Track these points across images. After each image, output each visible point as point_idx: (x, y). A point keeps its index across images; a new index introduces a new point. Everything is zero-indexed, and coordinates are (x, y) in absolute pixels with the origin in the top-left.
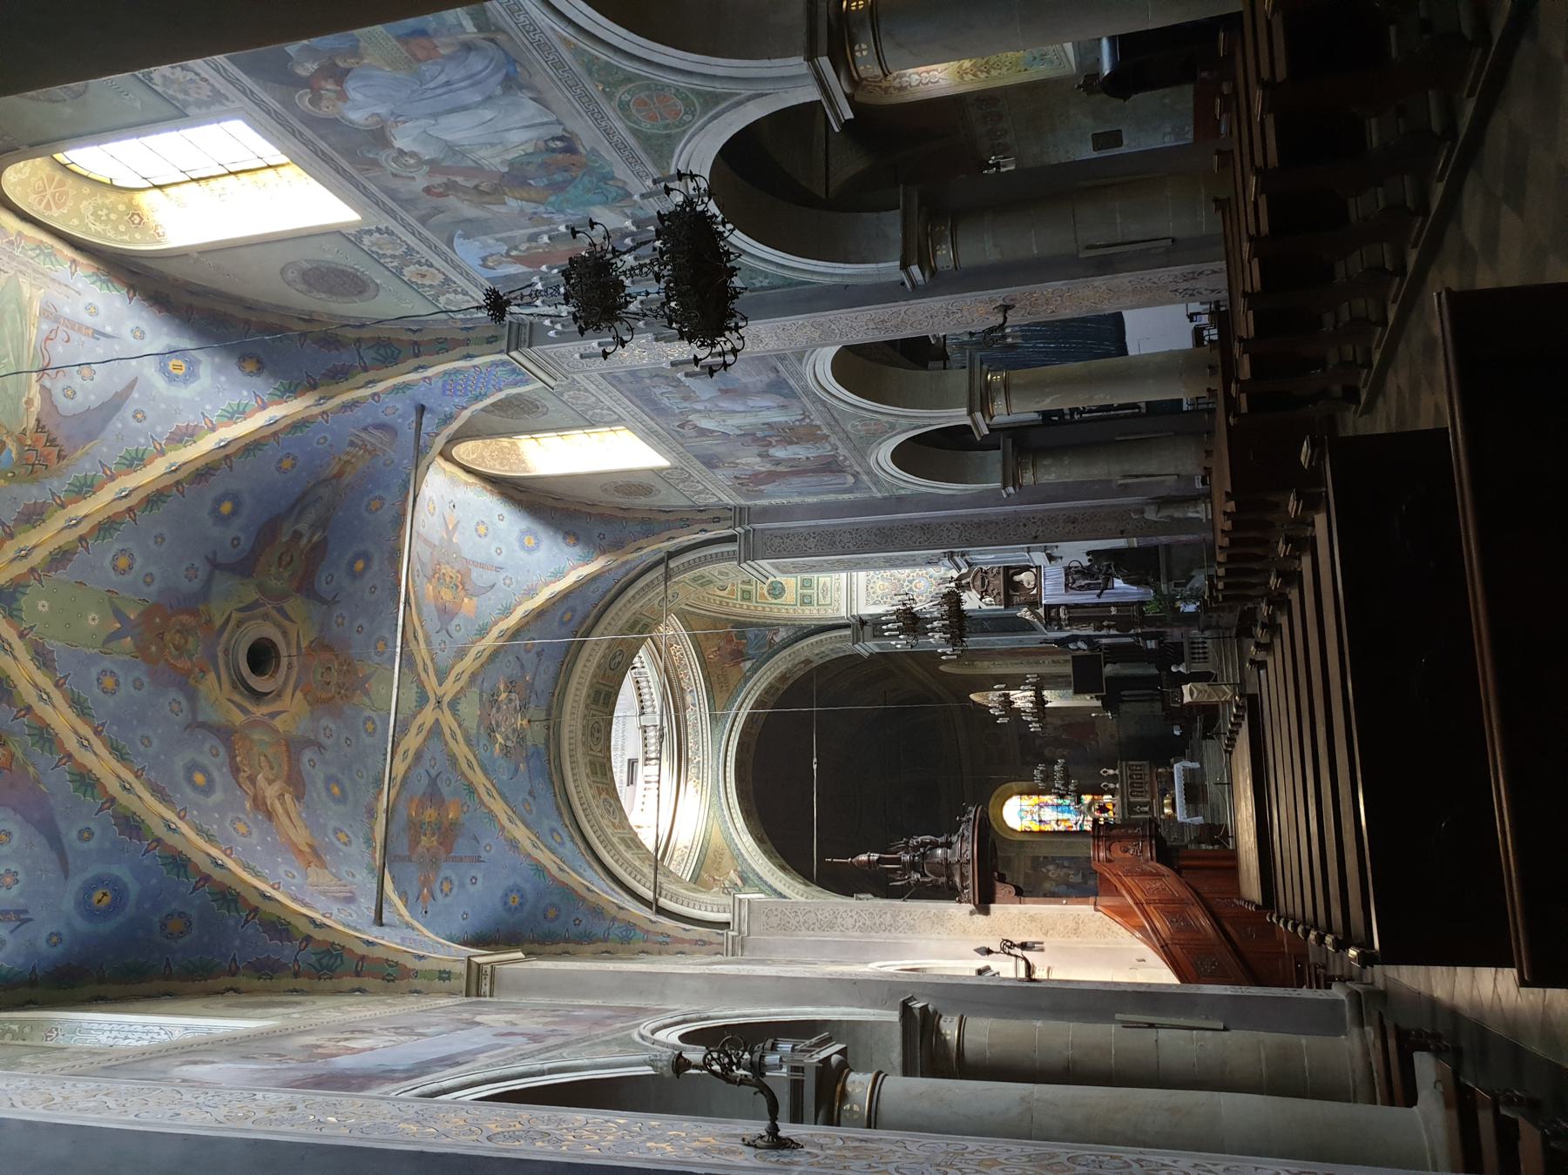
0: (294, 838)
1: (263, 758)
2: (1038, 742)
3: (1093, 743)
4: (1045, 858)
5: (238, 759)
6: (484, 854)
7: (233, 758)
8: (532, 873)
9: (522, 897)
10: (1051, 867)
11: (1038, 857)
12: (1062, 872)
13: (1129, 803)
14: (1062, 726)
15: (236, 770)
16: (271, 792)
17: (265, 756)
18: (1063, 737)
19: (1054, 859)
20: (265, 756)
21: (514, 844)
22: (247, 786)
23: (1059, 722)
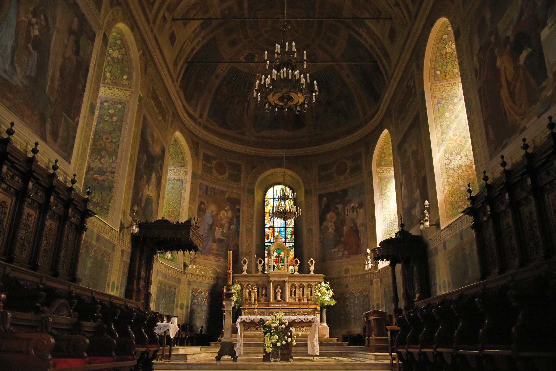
2: (340, 207)
3: (340, 254)
4: (239, 210)
10: (230, 214)
11: (239, 204)
12: (225, 222)
13: (284, 282)
14: (356, 225)
18: (345, 228)
19: (238, 217)
23: (359, 222)
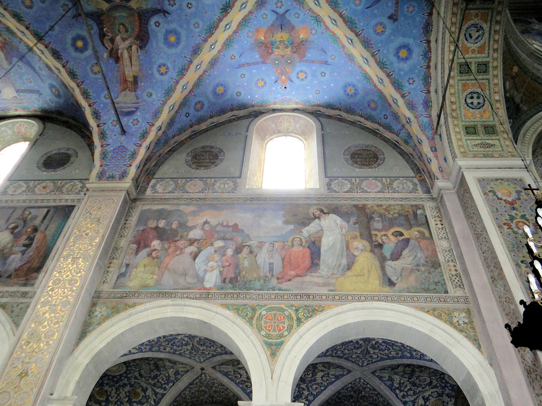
0: (126, 72)
1: (121, 26)
5: (105, 29)
6: (330, 61)
7: (101, 29)
8: (362, 78)
9: (356, 90)
15: (102, 36)
16: (122, 45)
17: (123, 25)
20: (123, 25)
21: (351, 58)
22: (108, 45)
